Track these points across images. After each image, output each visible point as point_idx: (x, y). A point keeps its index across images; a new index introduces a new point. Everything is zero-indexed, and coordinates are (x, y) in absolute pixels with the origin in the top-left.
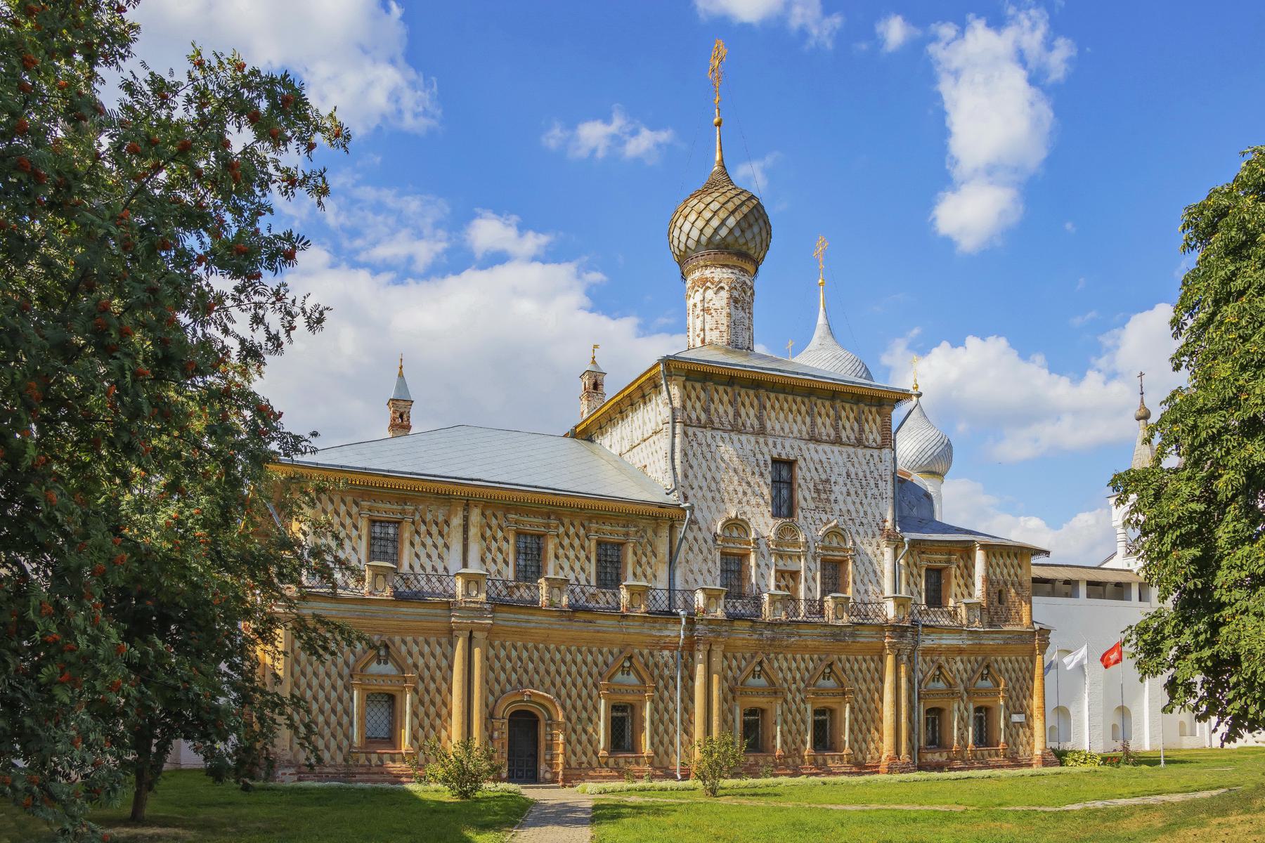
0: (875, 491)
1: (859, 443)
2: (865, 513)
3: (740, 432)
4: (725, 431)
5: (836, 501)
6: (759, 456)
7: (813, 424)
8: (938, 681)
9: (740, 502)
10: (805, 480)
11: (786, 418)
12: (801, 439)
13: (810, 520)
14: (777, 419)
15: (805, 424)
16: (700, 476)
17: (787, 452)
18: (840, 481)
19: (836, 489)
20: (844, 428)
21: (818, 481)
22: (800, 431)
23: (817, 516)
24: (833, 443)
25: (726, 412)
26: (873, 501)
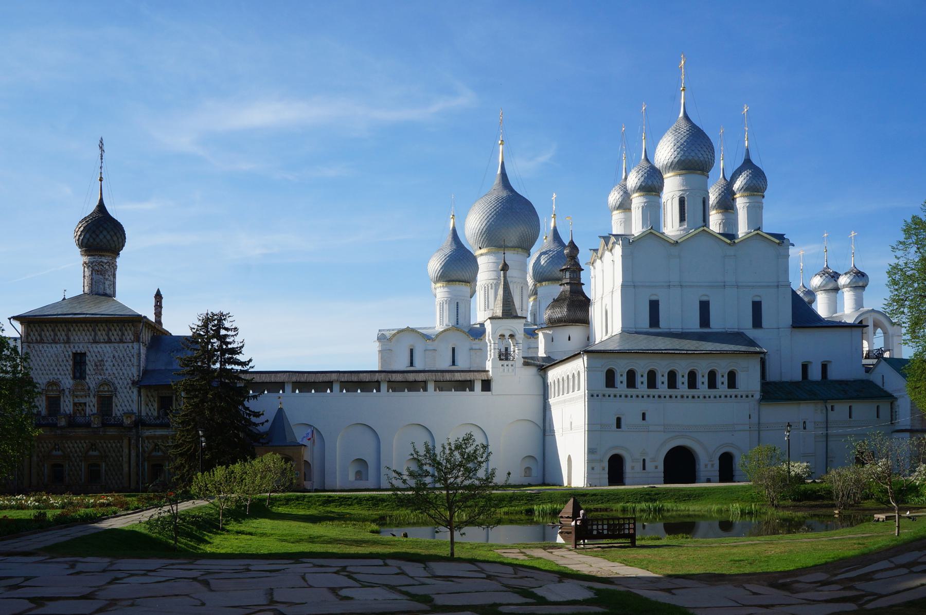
0: (130, 363)
1: (121, 341)
2: (123, 374)
3: (56, 343)
4: (49, 343)
5: (107, 370)
6: (66, 353)
7: (96, 334)
8: (158, 452)
9: (56, 374)
10: (90, 361)
11: (81, 334)
12: (89, 342)
13: (92, 379)
14: (76, 335)
15: (91, 335)
16: (36, 365)
17: (80, 348)
18: (109, 360)
19: (107, 364)
20: (113, 335)
21: (96, 360)
22: (89, 339)
23: (96, 377)
24: (106, 343)
25: (51, 336)
26: (128, 368)
